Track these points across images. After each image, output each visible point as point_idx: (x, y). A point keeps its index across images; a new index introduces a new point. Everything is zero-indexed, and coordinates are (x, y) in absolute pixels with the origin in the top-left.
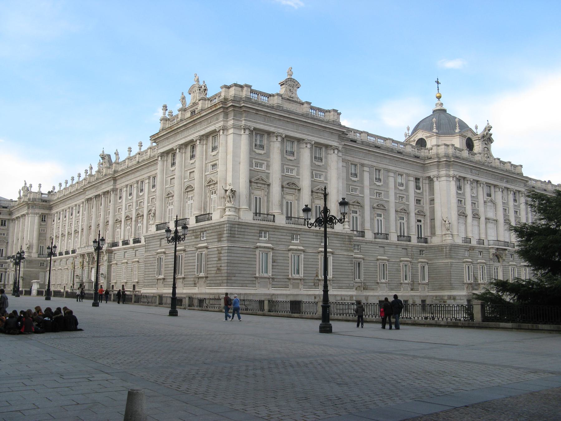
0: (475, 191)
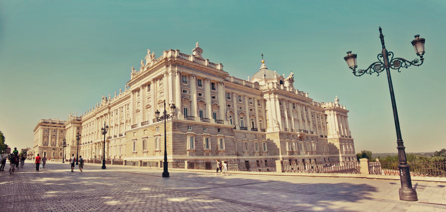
0: (287, 105)
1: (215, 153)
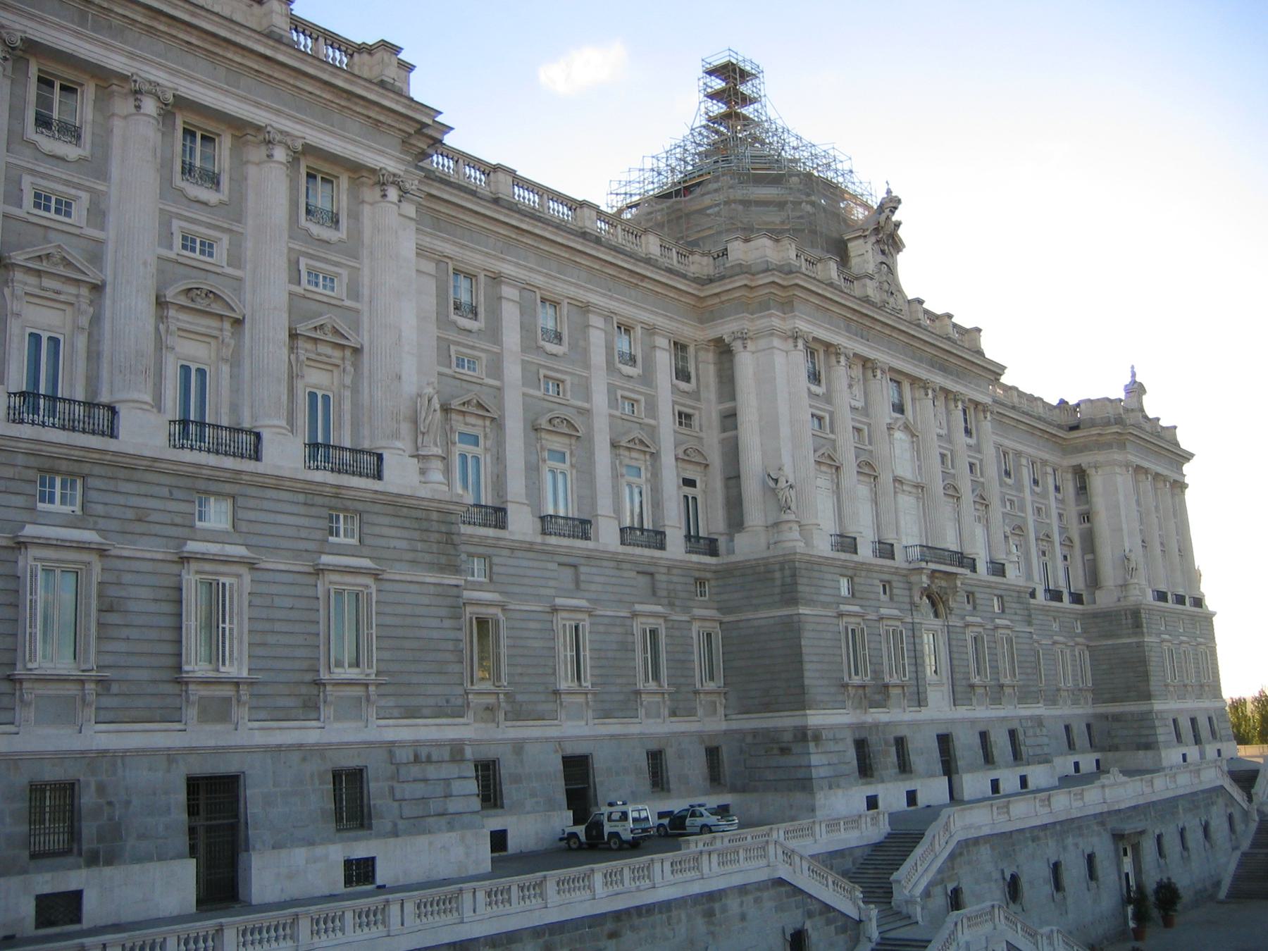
0: (858, 390)
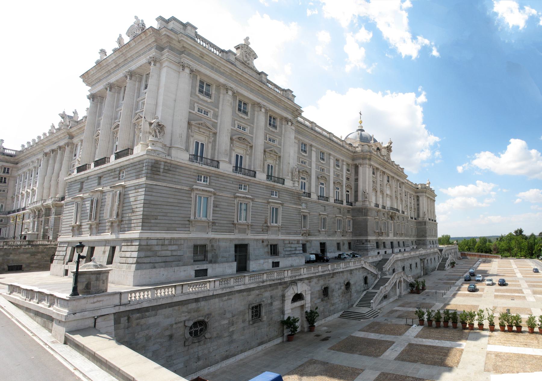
1: (261, 230)
